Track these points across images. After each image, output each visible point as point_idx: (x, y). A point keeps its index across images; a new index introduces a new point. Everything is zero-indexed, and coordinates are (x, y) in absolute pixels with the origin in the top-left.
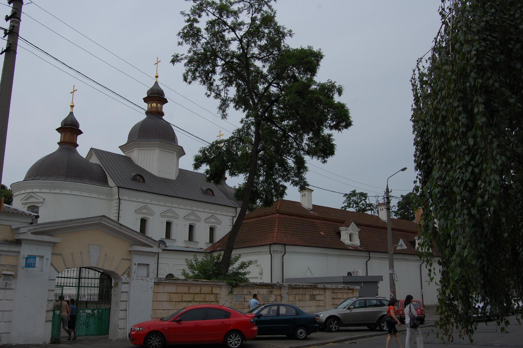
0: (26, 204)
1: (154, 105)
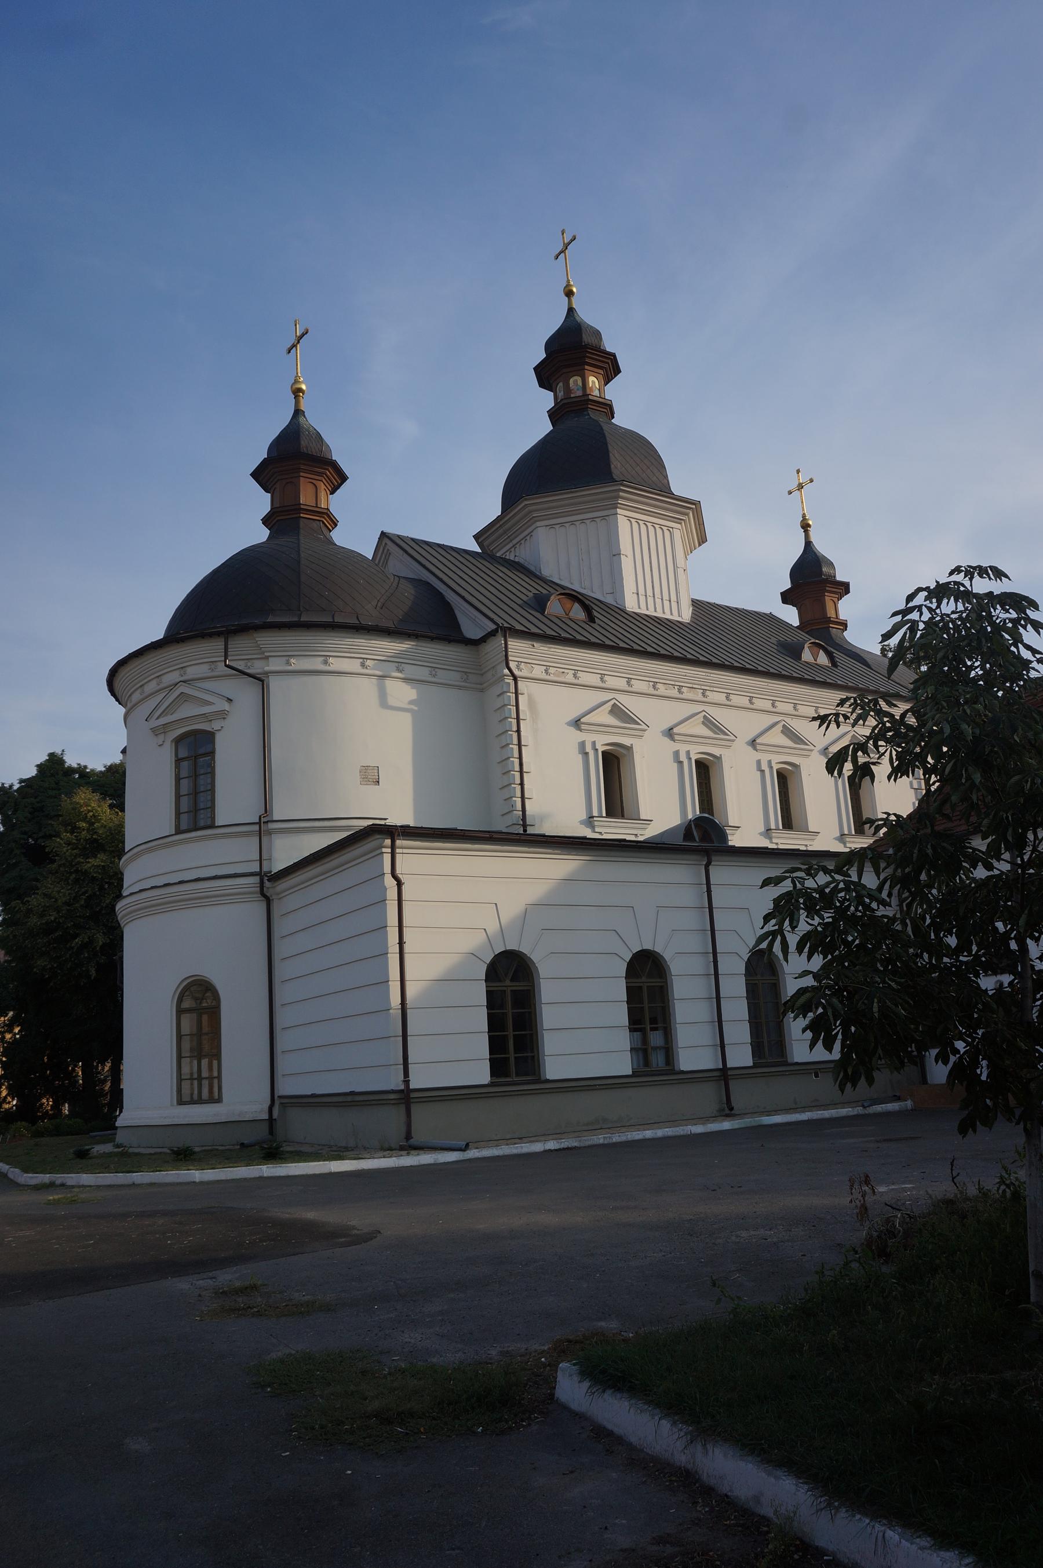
0: (164, 729)
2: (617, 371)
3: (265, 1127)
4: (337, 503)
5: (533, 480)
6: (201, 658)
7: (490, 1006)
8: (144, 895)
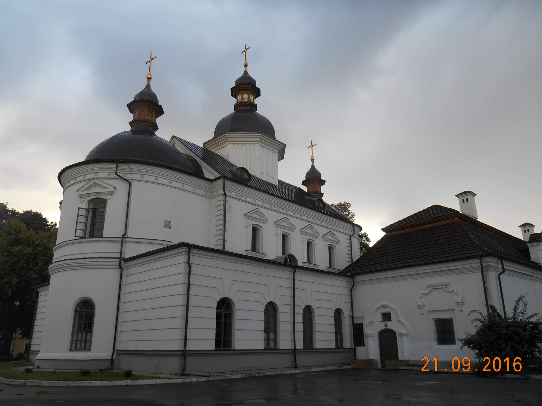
0: (86, 195)
1: (246, 96)
2: (259, 95)
3: (109, 363)
4: (159, 121)
5: (227, 128)
6: (104, 171)
7: (217, 319)
8: (66, 262)
